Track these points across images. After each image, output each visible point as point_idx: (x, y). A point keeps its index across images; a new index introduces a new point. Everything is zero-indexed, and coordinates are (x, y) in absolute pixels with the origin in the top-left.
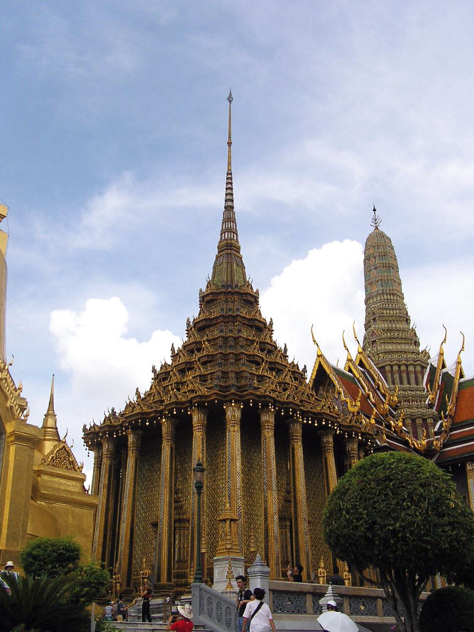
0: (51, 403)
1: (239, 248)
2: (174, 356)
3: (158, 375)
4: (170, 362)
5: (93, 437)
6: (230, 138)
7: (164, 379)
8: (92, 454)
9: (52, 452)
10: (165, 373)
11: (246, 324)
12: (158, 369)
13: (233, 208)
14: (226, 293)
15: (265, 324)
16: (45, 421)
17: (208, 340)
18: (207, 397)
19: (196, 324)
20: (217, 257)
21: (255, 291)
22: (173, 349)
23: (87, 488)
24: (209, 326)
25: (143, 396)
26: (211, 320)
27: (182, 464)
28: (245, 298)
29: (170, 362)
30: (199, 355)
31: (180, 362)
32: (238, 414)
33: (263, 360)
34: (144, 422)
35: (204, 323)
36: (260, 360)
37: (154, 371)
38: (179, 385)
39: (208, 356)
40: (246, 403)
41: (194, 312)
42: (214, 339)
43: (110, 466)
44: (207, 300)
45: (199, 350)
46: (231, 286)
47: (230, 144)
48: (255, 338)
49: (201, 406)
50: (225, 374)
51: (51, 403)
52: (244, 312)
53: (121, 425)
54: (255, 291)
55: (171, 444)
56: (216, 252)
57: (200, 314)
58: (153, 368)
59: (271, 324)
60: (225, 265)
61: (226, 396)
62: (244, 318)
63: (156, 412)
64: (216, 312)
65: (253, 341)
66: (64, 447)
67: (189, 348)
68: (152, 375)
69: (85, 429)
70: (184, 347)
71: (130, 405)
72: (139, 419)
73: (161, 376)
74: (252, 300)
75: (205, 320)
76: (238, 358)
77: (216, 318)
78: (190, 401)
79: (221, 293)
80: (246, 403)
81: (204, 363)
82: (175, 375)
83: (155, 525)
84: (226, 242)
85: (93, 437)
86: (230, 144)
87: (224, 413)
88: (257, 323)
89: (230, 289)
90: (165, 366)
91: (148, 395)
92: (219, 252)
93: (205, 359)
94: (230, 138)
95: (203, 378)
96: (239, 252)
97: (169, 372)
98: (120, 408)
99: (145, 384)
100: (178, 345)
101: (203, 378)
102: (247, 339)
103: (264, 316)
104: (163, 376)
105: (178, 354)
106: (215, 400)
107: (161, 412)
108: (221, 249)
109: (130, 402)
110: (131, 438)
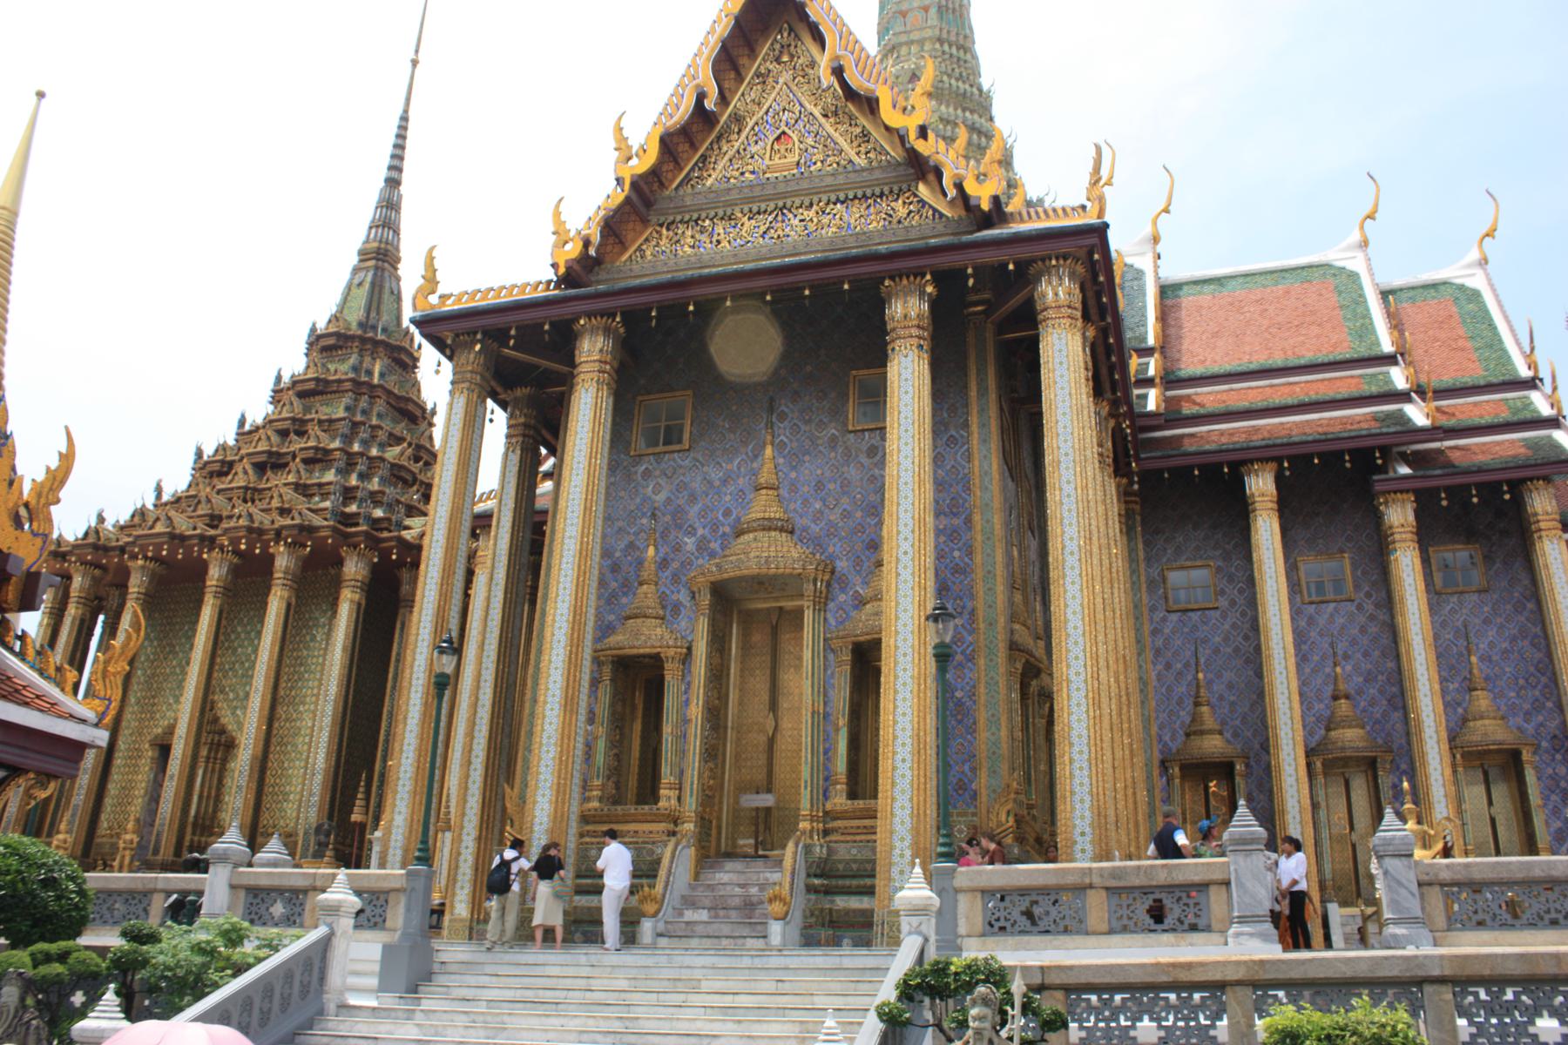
1: (398, 260)
2: (244, 435)
3: (207, 463)
4: (231, 442)
6: (417, 51)
7: (222, 474)
10: (223, 462)
12: (208, 451)
14: (363, 340)
15: (424, 410)
17: (320, 422)
19: (295, 382)
20: (356, 270)
22: (242, 422)
24: (322, 393)
25: (165, 498)
26: (327, 382)
29: (231, 442)
30: (297, 444)
31: (259, 449)
33: (415, 480)
35: (312, 385)
36: (409, 478)
37: (199, 453)
38: (251, 494)
39: (316, 449)
40: (384, 555)
41: (295, 363)
42: (331, 421)
43: (82, 621)
44: (325, 344)
46: (374, 328)
47: (415, 63)
49: (297, 544)
52: (392, 382)
53: (122, 550)
56: (354, 259)
57: (308, 367)
60: (367, 286)
62: (389, 393)
64: (341, 369)
67: (280, 425)
70: (269, 422)
71: (141, 513)
73: (213, 468)
75: (317, 380)
77: (339, 381)
78: (278, 533)
79: (352, 338)
80: (384, 555)
81: (306, 461)
82: (246, 472)
83: (164, 750)
84: (376, 245)
86: (415, 63)
87: (340, 562)
88: (411, 407)
89: (370, 335)
90: (223, 448)
91: (177, 501)
92: (361, 261)
93: (310, 454)
94: (417, 51)
96: (396, 269)
97: (231, 464)
101: (302, 489)
104: (216, 467)
105: (250, 432)
106: (327, 538)
107: (212, 539)
108: (364, 255)
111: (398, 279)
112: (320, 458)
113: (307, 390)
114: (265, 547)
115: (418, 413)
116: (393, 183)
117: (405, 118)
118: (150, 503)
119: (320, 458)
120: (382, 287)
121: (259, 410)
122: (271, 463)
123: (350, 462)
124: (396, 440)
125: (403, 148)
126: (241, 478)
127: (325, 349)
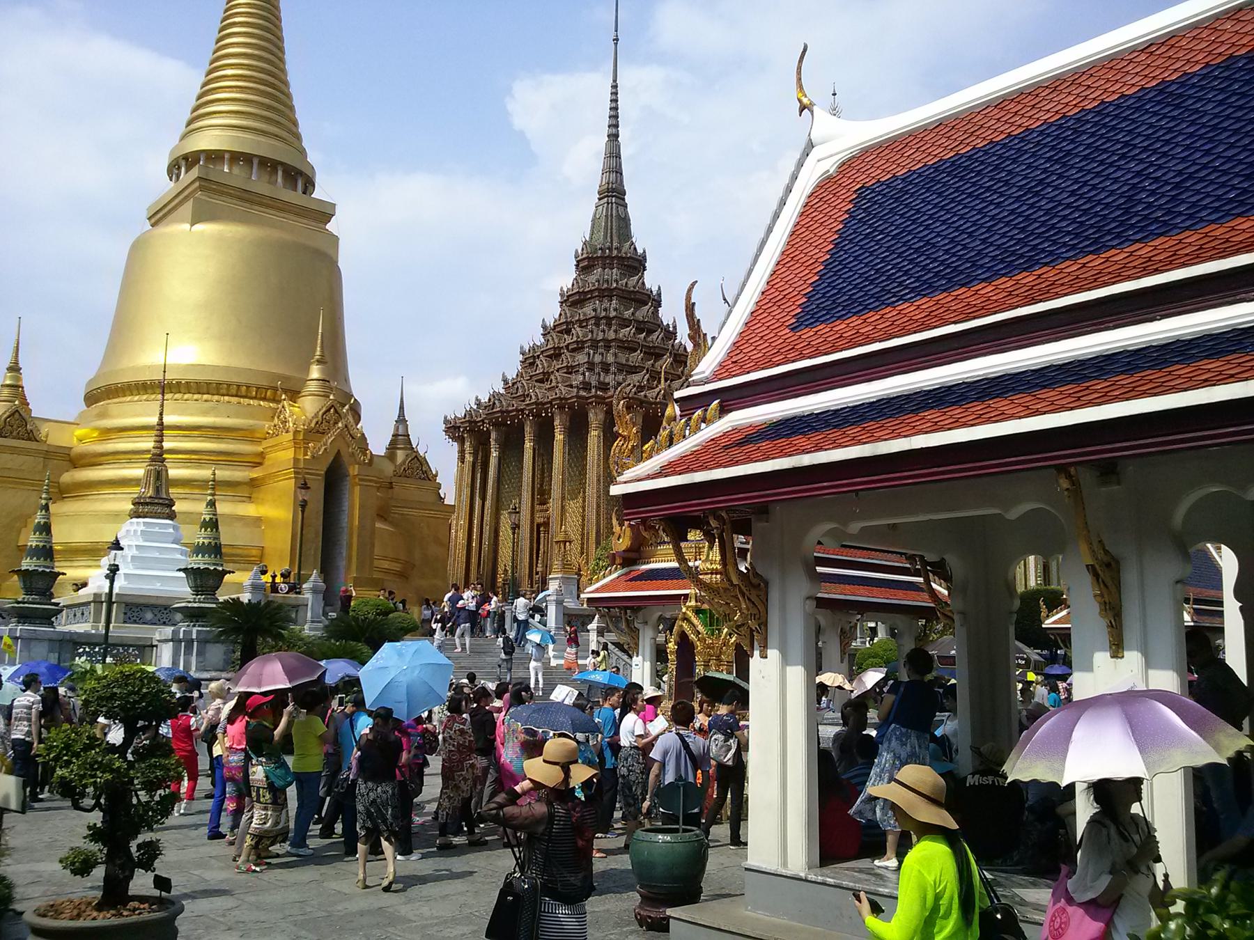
0: (402, 408)
4: (539, 340)
5: (454, 430)
7: (532, 364)
8: (455, 444)
9: (404, 462)
13: (617, 136)
16: (397, 429)
21: (640, 251)
22: (544, 327)
30: (569, 339)
34: (505, 420)
41: (566, 278)
42: (587, 320)
44: (586, 264)
45: (568, 332)
49: (561, 407)
50: (591, 366)
51: (402, 408)
58: (522, 348)
59: (659, 295)
63: (517, 410)
68: (521, 358)
69: (446, 421)
73: (530, 360)
74: (636, 264)
76: (607, 344)
78: (550, 402)
81: (574, 350)
85: (454, 430)
90: (533, 348)
95: (570, 370)
98: (484, 399)
99: (513, 368)
100: (550, 323)
103: (648, 286)
107: (522, 410)
110: (493, 435)
111: (625, 206)
112: (579, 347)
113: (573, 300)
115: (645, 298)
116: (614, 137)
117: (615, 87)
119: (579, 347)
121: (552, 312)
122: (556, 354)
123: (595, 344)
124: (625, 323)
125: (616, 109)
126: (542, 364)
127: (584, 268)
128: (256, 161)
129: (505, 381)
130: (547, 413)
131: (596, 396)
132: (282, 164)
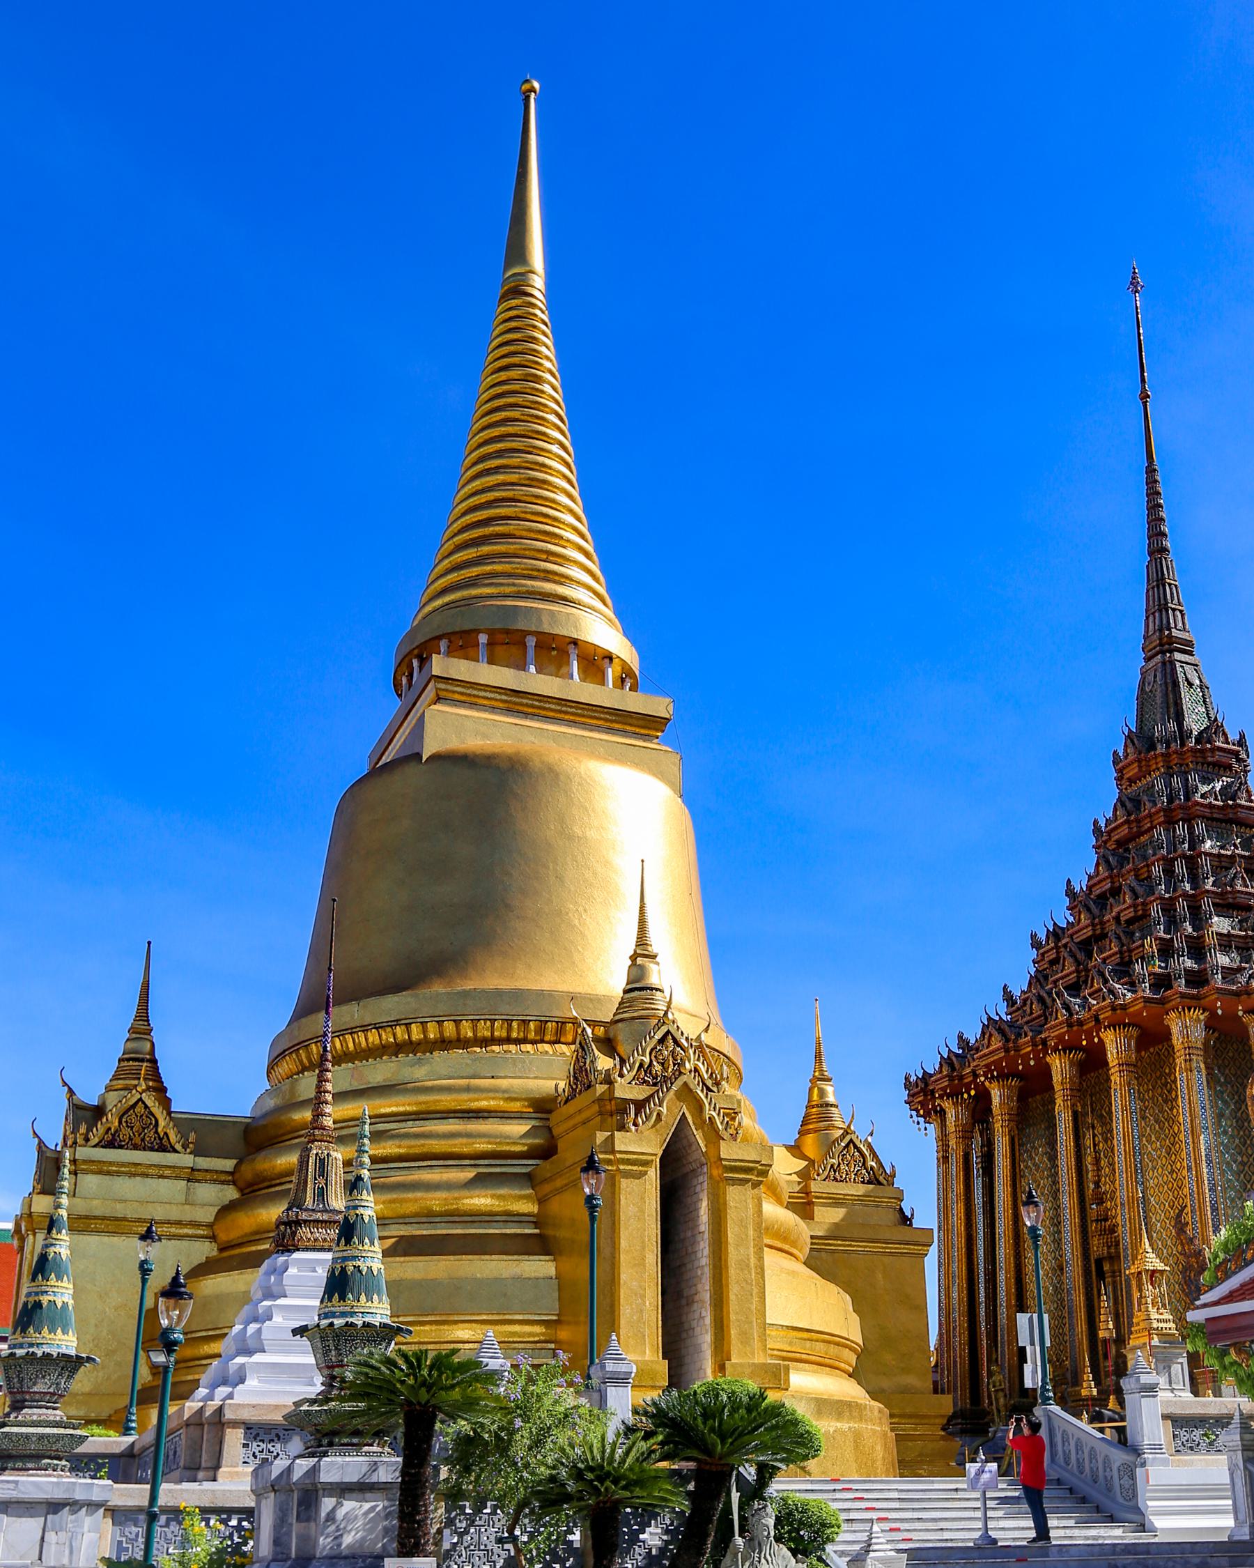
8: (932, 1128)
11: (1217, 820)
18: (1124, 1007)
21: (1233, 736)
22: (1070, 893)
23: (908, 1214)
27: (1106, 1140)
28: (1210, 759)
32: (1198, 1034)
48: (1239, 851)
54: (1233, 736)
55: (1073, 1105)
61: (1162, 1002)
62: (1210, 806)
65: (1233, 856)
66: (851, 1141)
72: (1001, 1060)
85: (922, 1096)
90: (1056, 934)
102: (1220, 855)
109: (989, 1019)
110: (996, 1101)
114: (1090, 1039)
118: (1001, 1011)
120: (1176, 684)
128: (531, 642)
129: (1008, 997)
130: (1090, 1039)
131: (1183, 995)
132: (575, 642)
